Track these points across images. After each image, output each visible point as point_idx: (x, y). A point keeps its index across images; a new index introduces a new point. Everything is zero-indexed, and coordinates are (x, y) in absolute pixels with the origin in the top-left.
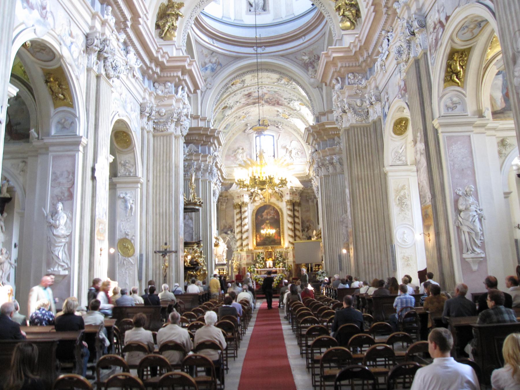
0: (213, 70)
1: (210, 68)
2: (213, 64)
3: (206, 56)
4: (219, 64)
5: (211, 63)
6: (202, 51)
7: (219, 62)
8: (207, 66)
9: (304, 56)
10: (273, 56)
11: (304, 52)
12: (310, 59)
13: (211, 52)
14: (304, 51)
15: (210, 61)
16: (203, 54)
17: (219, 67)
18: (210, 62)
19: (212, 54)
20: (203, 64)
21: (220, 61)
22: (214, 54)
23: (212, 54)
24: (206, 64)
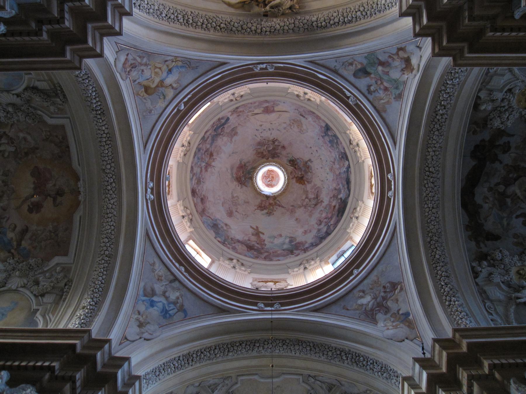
0: (165, 313)
1: (160, 305)
2: (170, 303)
3: (159, 279)
4: (182, 309)
5: (167, 298)
6: (154, 264)
7: (183, 305)
8: (155, 299)
9: (362, 297)
10: (296, 311)
11: (360, 291)
12: (375, 298)
13: (172, 277)
14: (360, 288)
15: (164, 293)
16: (153, 271)
17: (181, 315)
18: (164, 294)
19: (171, 282)
20: (149, 290)
21: (187, 305)
22: (176, 284)
23: (171, 282)
24: (153, 293)
